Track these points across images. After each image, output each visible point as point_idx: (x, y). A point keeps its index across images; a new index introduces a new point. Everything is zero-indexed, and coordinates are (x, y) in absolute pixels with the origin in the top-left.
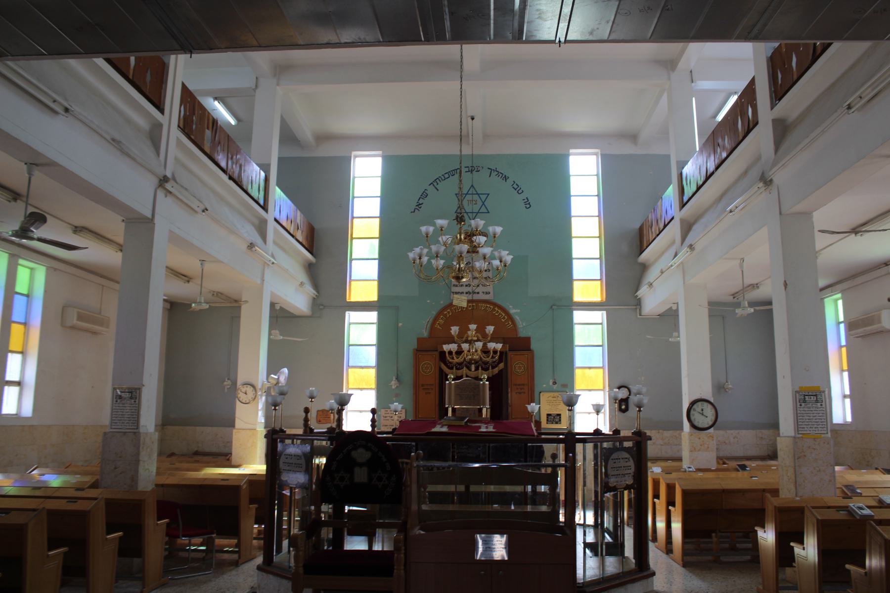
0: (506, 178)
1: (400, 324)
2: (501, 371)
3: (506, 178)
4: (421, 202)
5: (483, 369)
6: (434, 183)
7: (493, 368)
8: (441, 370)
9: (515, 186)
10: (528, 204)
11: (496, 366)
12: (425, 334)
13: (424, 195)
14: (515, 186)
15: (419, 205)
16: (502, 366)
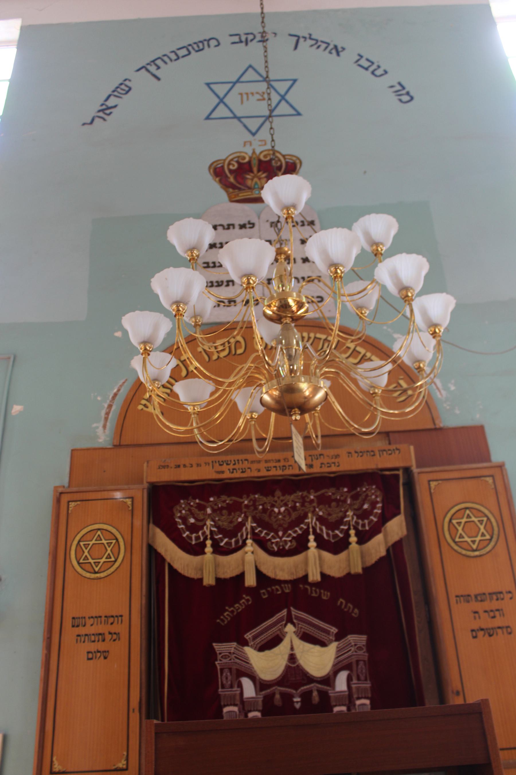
0: (337, 51)
1: (16, 409)
2: (396, 548)
3: (337, 51)
4: (111, 102)
5: (322, 544)
6: (151, 68)
7: (363, 538)
8: (155, 559)
9: (366, 64)
10: (403, 94)
11: (376, 530)
12: (103, 436)
13: (123, 89)
14: (366, 64)
15: (106, 110)
16: (396, 527)
